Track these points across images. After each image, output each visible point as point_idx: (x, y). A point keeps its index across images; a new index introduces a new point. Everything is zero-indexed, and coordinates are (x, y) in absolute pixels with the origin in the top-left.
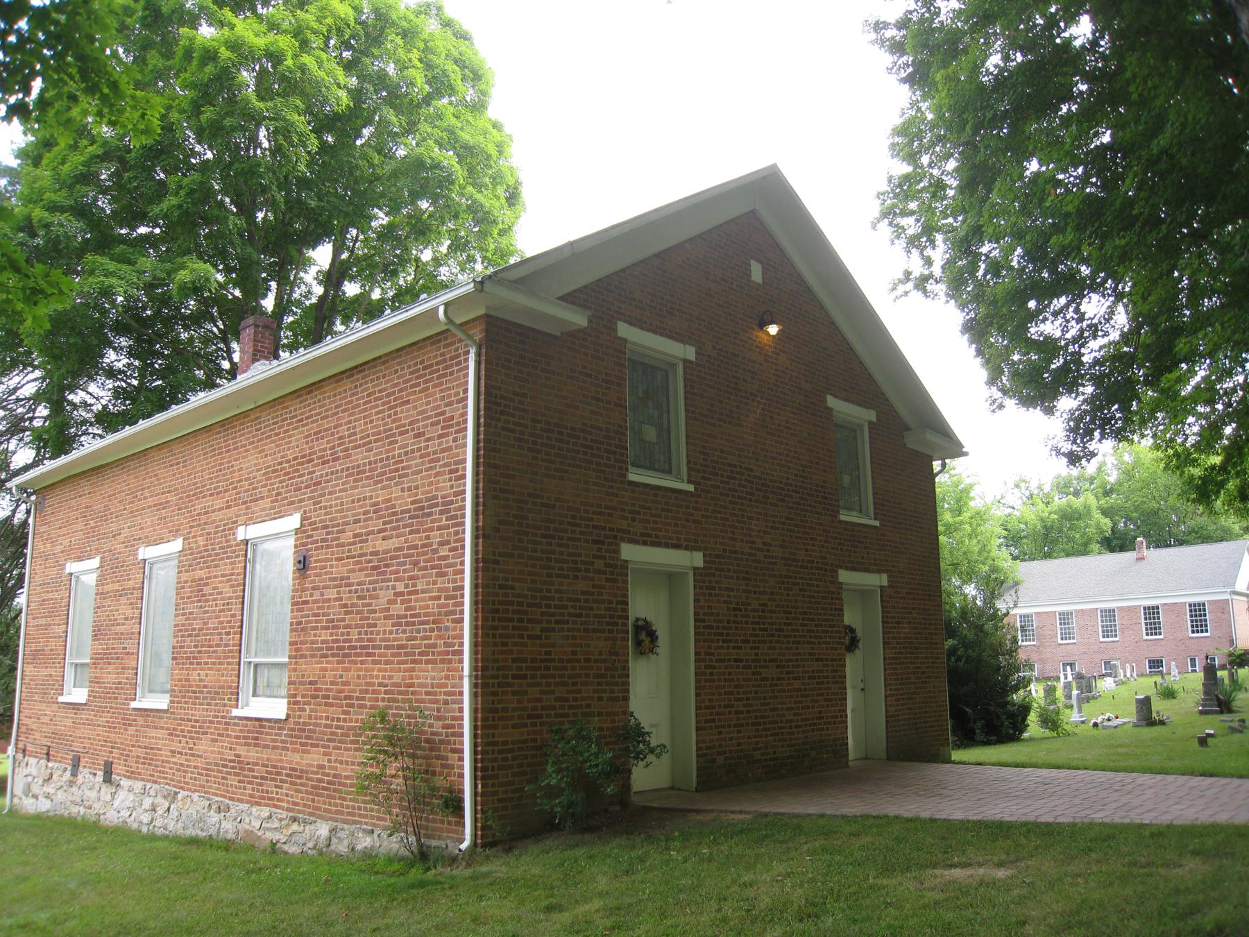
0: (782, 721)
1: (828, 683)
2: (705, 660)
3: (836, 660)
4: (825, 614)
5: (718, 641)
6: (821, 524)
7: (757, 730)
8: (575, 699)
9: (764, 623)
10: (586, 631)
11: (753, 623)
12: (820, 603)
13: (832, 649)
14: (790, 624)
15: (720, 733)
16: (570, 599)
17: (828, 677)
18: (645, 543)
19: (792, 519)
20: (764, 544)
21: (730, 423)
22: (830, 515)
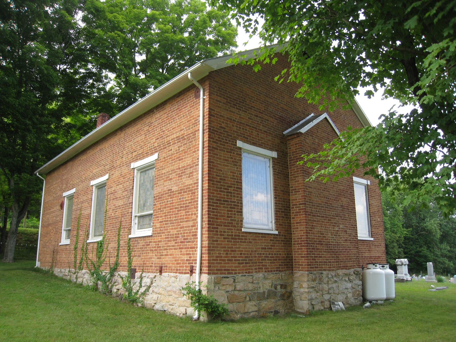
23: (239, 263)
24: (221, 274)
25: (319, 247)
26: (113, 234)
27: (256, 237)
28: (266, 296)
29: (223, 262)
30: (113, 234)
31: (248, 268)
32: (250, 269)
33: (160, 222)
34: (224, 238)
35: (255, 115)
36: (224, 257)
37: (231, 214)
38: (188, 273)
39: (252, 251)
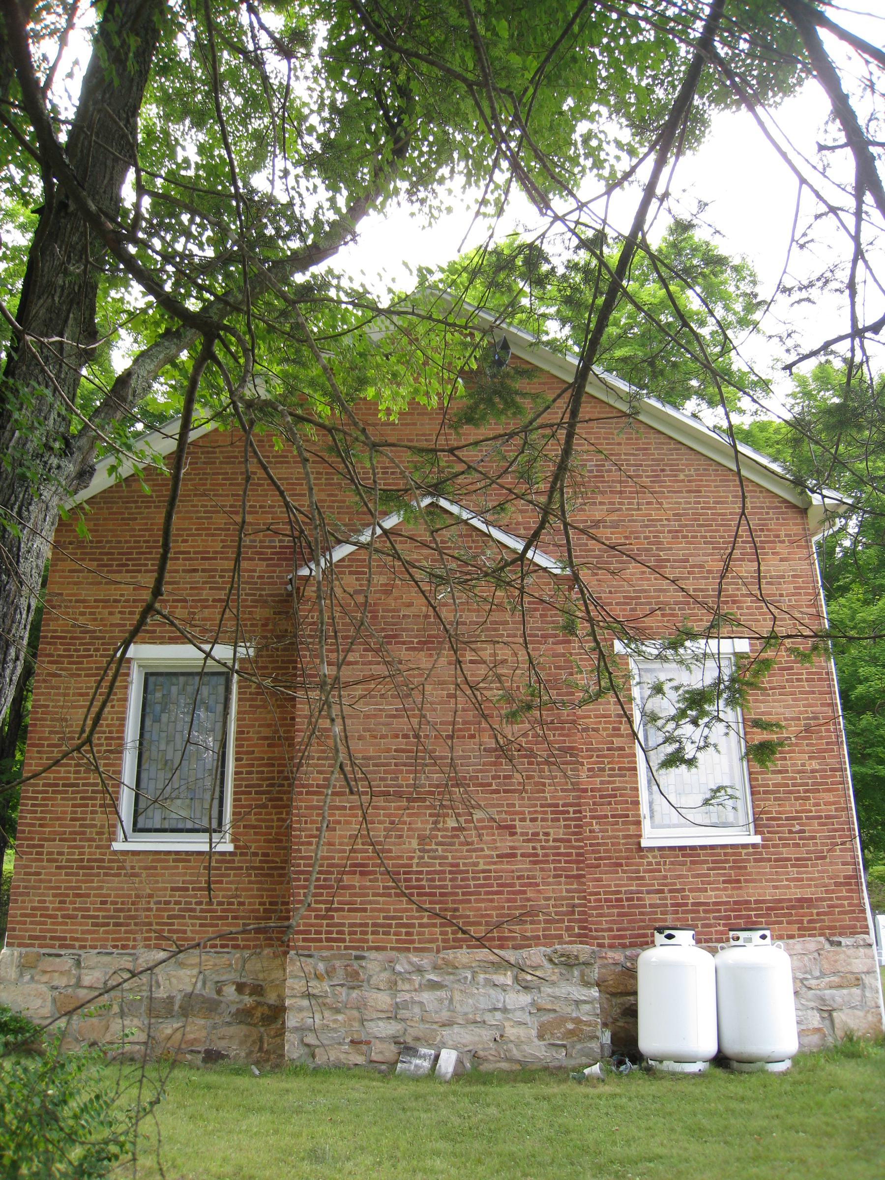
23: (95, 925)
24: (41, 946)
25: (356, 881)
27: (153, 861)
28: (176, 1007)
29: (49, 920)
31: (123, 935)
32: (128, 939)
34: (58, 868)
35: (184, 571)
36: (54, 909)
37: (85, 812)
39: (137, 896)
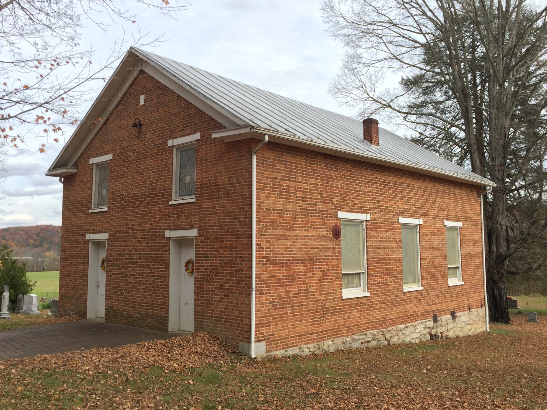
0: (135, 302)
1: (158, 287)
2: (109, 273)
3: (163, 277)
4: (158, 254)
5: (113, 266)
6: (160, 209)
7: (125, 303)
8: (76, 284)
9: (130, 259)
10: (79, 263)
11: (126, 259)
12: (156, 249)
13: (161, 271)
14: (141, 259)
15: (112, 302)
16: (76, 254)
17: (158, 285)
18: (93, 233)
19: (145, 211)
20: (132, 225)
21: (123, 178)
22: (165, 204)
26: (433, 283)
30: (433, 283)
33: (467, 275)
38: (480, 307)
